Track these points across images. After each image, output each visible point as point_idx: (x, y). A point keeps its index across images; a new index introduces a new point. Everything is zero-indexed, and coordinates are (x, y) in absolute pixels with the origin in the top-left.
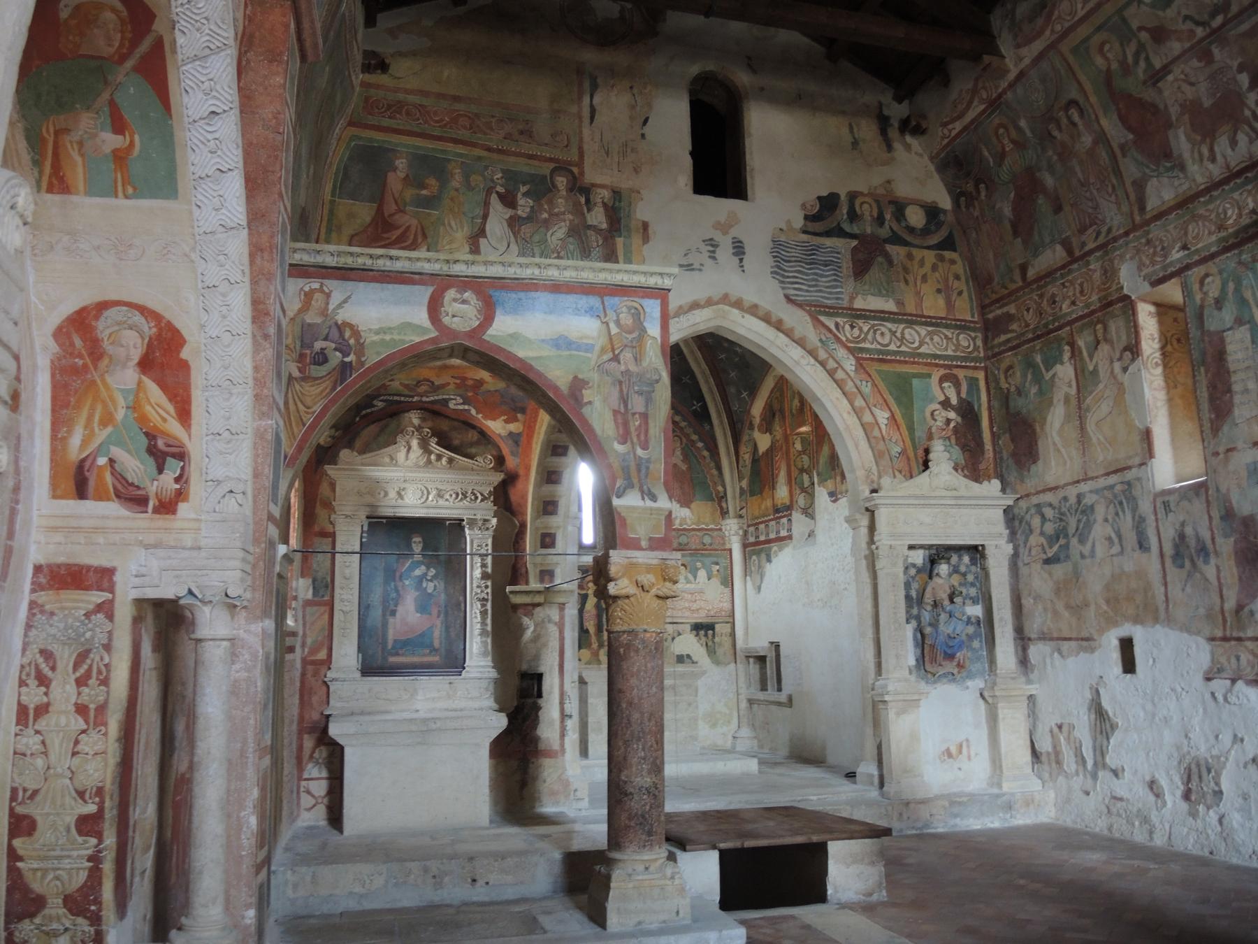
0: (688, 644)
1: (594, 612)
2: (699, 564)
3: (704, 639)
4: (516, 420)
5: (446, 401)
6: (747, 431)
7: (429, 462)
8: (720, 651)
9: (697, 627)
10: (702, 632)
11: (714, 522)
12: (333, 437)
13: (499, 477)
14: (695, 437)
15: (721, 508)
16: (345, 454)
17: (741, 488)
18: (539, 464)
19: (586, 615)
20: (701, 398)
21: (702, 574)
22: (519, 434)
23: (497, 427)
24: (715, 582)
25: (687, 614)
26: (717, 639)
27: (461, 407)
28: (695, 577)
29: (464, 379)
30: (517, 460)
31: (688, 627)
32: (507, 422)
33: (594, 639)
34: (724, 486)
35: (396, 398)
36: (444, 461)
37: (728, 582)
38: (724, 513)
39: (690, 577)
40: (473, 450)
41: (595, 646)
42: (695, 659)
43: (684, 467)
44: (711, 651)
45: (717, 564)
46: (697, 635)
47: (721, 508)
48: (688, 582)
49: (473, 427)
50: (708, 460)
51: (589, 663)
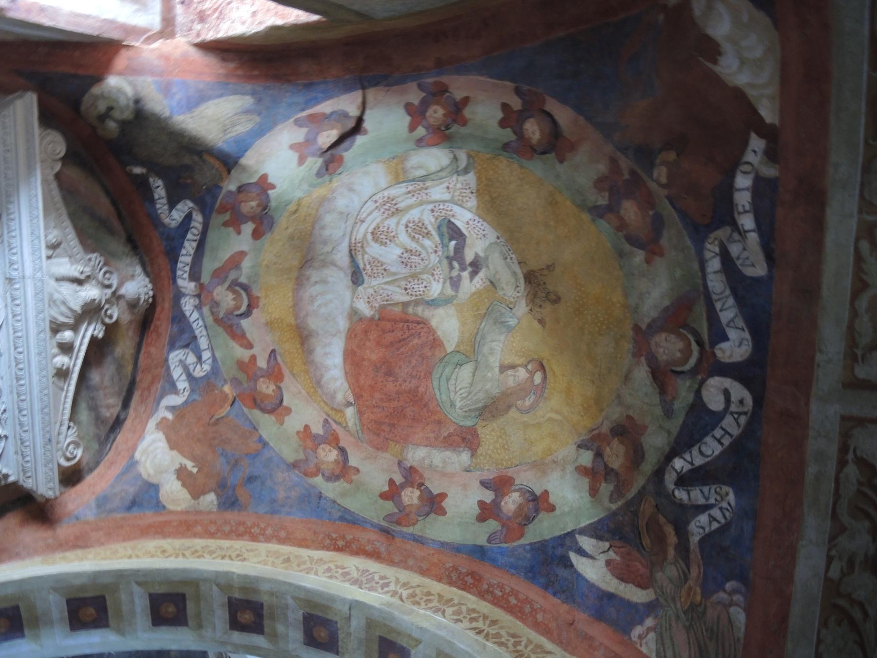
4: (196, 493)
5: (191, 343)
7: (56, 328)
12: (104, 117)
13: (43, 484)
16: (58, 145)
18: (121, 576)
22: (159, 506)
23: (153, 452)
27: (177, 373)
29: (275, 374)
30: (90, 515)
32: (181, 473)
35: (189, 247)
36: (61, 360)
40: (84, 415)
49: (126, 404)
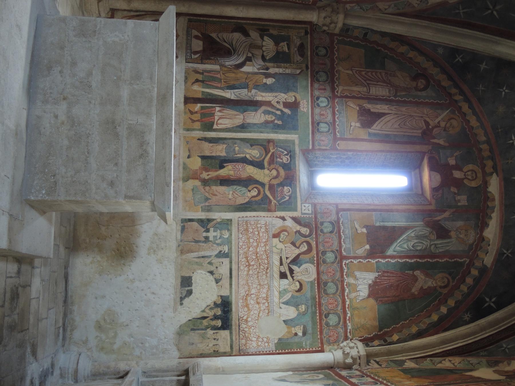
0: (206, 294)
1: (244, 175)
2: (303, 308)
3: (211, 314)
6: (484, 360)
8: (195, 336)
9: (225, 305)
10: (219, 312)
11: (355, 329)
14: (451, 303)
15: (372, 339)
17: (404, 361)
19: (240, 166)
20: (500, 306)
21: (291, 313)
24: (282, 331)
25: (242, 292)
26: (210, 332)
28: (286, 303)
31: (225, 293)
33: (213, 174)
34: (399, 341)
37: (283, 347)
38: (366, 341)
39: (287, 297)
41: (205, 175)
42: (186, 301)
43: (415, 290)
44: (195, 325)
45: (304, 333)
46: (216, 305)
47: (372, 339)
48: (282, 293)
50: (428, 321)
51: (185, 167)
